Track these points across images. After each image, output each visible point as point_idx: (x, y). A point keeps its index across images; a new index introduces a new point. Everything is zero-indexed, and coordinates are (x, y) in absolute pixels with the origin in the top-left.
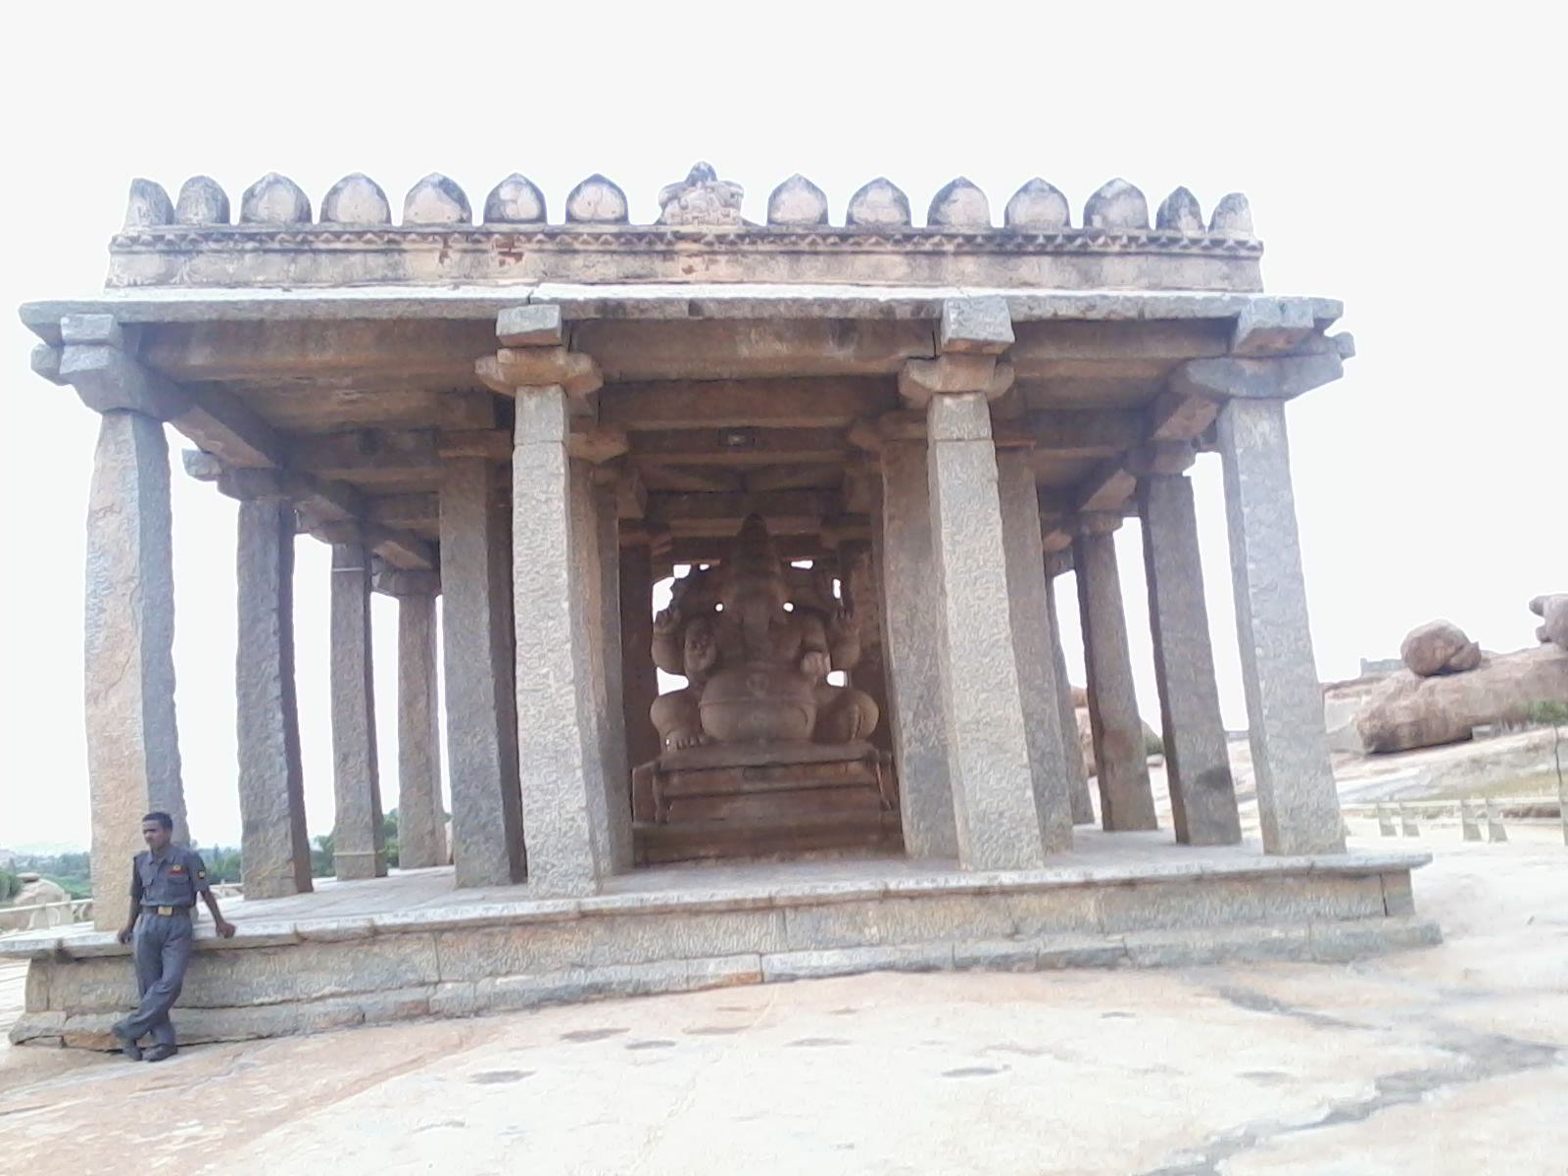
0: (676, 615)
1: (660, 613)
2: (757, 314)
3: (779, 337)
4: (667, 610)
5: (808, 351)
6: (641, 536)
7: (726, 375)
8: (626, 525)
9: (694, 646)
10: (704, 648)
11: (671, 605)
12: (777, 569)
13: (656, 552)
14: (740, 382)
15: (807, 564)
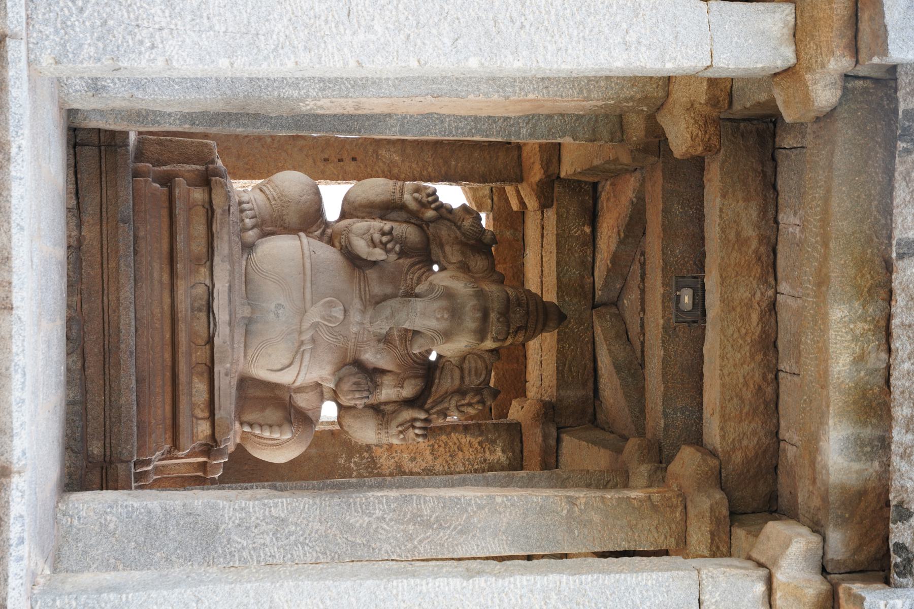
0: (430, 214)
1: (434, 193)
2: (896, 331)
3: (859, 359)
4: (437, 199)
5: (836, 399)
6: (536, 174)
7: (784, 287)
8: (553, 153)
9: (390, 233)
10: (385, 245)
11: (442, 206)
12: (489, 344)
13: (509, 190)
14: (773, 306)
15: (492, 384)
